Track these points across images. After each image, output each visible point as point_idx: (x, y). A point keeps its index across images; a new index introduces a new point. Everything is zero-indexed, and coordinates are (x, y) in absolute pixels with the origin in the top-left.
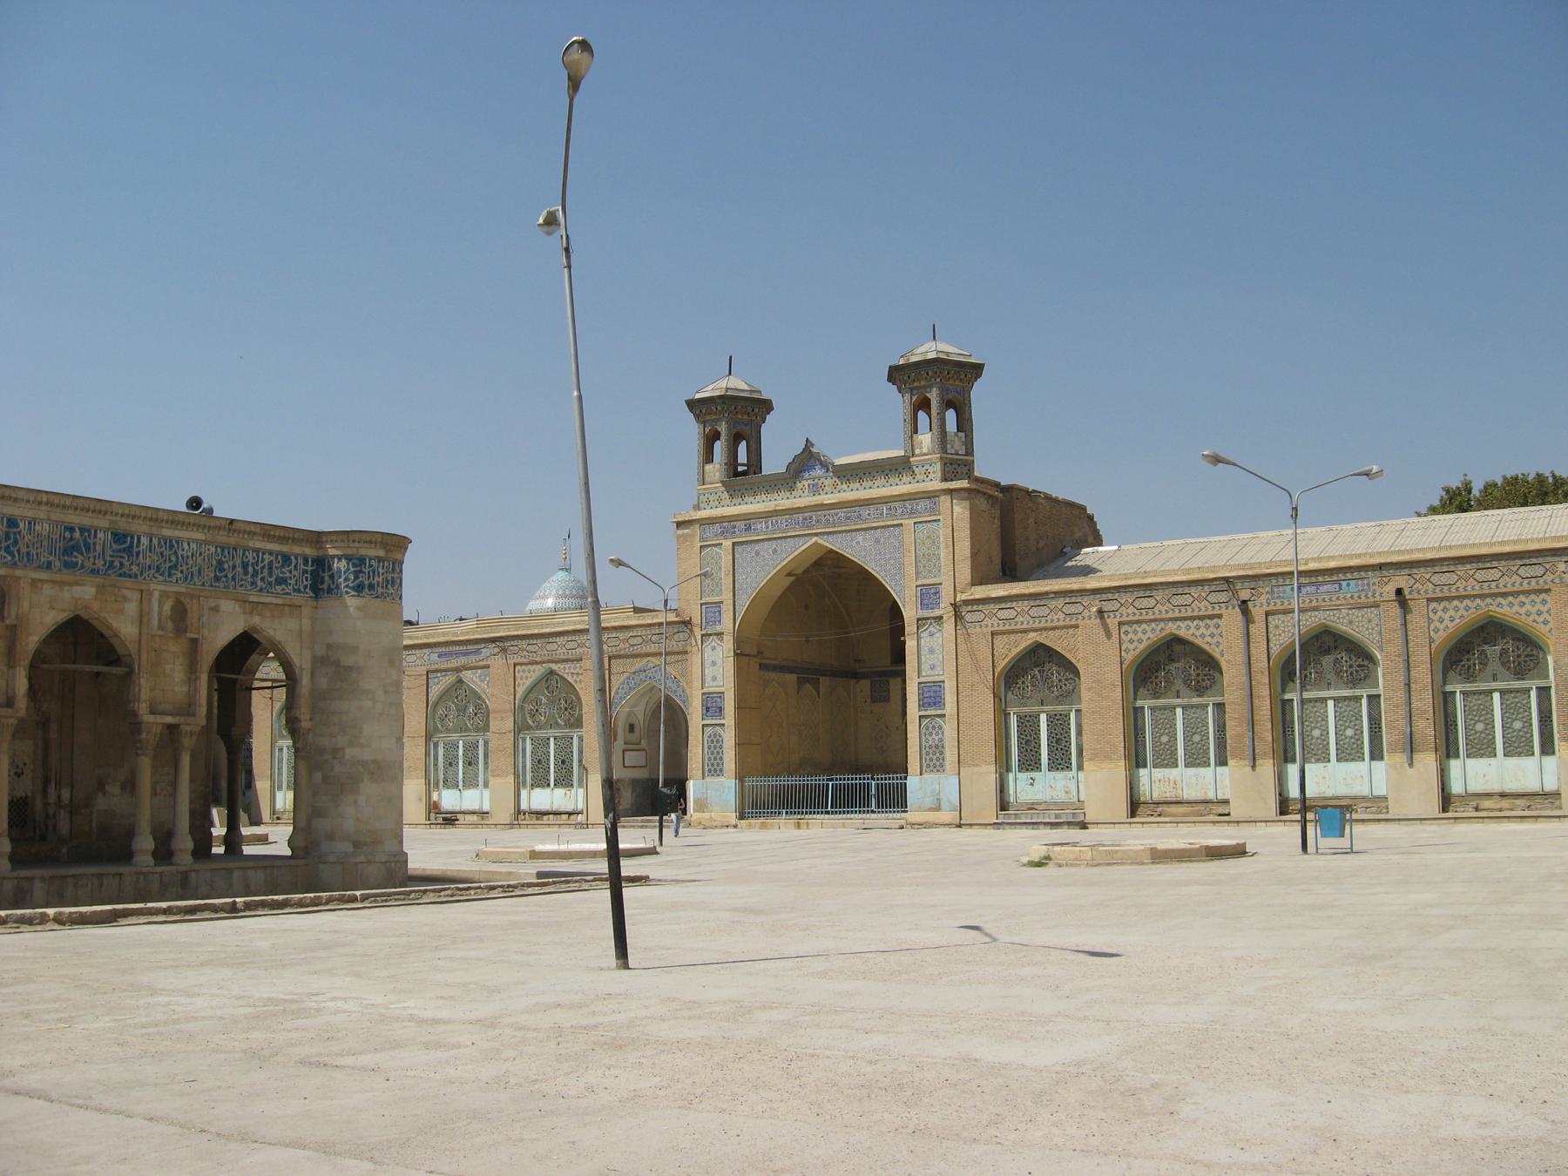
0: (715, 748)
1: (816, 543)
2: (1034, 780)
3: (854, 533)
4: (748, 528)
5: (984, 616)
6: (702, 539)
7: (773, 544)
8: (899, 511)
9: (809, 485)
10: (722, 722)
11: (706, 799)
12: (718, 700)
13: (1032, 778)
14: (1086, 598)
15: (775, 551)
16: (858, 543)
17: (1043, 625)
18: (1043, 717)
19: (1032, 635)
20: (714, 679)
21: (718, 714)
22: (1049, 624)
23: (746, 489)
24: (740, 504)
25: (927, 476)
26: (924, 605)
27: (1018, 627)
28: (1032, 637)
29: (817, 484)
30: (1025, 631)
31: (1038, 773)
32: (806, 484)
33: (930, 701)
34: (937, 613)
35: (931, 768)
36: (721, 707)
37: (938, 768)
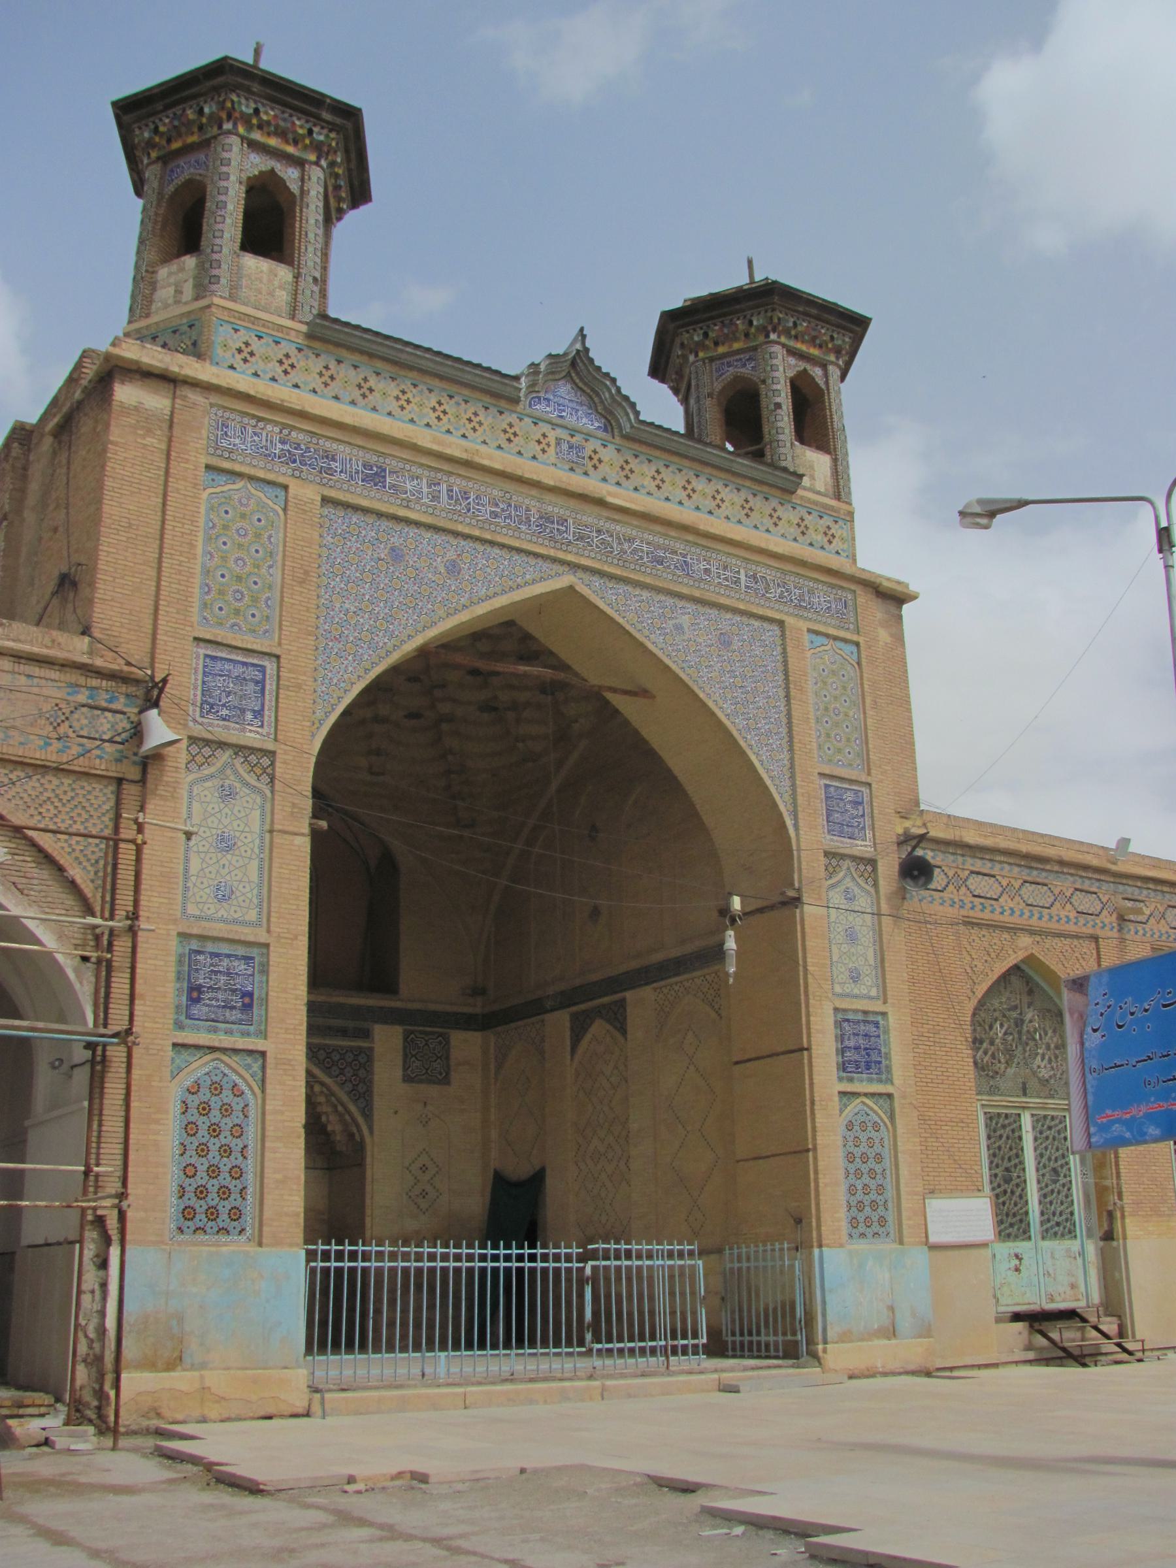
0: (215, 1130)
1: (571, 588)
2: (1021, 1260)
3: (670, 601)
4: (376, 477)
5: (946, 880)
6: (215, 448)
7: (452, 549)
8: (774, 593)
9: (559, 441)
10: (259, 1044)
11: (181, 1319)
12: (240, 967)
13: (1017, 1256)
14: (1105, 886)
15: (453, 569)
16: (679, 628)
17: (1044, 924)
18: (1026, 1121)
19: (1025, 941)
20: (224, 895)
21: (236, 1015)
22: (1053, 926)
23: (378, 374)
24: (353, 403)
25: (830, 542)
26: (836, 827)
27: (1006, 918)
28: (1023, 946)
29: (580, 448)
30: (1014, 930)
31: (1025, 1244)
32: (552, 436)
33: (856, 1057)
34: (862, 847)
35: (862, 1228)
36: (250, 995)
37: (876, 1227)
